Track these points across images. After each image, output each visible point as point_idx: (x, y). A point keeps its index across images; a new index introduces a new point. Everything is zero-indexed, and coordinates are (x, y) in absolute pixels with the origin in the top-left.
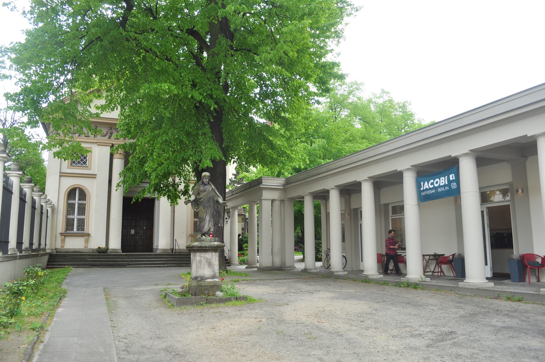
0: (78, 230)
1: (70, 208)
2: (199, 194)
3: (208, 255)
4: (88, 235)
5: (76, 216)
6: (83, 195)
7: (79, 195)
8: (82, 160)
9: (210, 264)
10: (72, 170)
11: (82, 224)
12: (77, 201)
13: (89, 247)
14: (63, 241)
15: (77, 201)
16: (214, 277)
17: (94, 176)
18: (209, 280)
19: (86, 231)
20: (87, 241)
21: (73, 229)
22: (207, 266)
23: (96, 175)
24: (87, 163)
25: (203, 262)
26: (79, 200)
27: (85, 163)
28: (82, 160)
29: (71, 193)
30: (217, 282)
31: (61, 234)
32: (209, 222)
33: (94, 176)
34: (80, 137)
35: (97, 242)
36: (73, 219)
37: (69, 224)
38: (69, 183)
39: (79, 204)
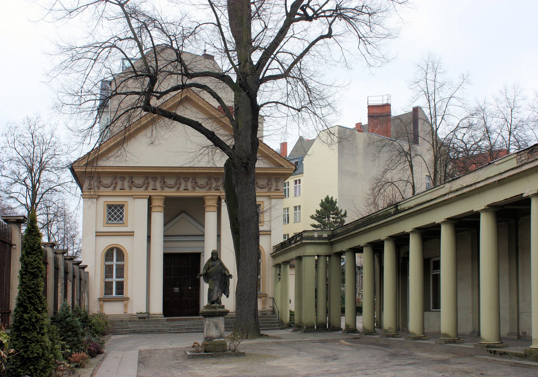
0: (118, 293)
1: (108, 271)
2: (209, 269)
3: (215, 320)
4: (127, 299)
5: (114, 279)
6: (121, 254)
7: (117, 256)
8: (118, 216)
9: (217, 327)
10: (108, 228)
11: (120, 287)
12: (115, 262)
13: (129, 312)
14: (101, 307)
15: (115, 262)
16: (221, 337)
17: (131, 234)
18: (216, 340)
19: (125, 295)
20: (126, 306)
21: (111, 293)
22: (214, 328)
23: (133, 232)
24: (124, 219)
25: (211, 326)
26: (117, 261)
27: (121, 219)
28: (118, 216)
29: (109, 254)
30: (222, 341)
31: (100, 300)
32: (218, 292)
33: (131, 234)
34: (115, 191)
36: (112, 283)
37: (108, 287)
38: (107, 242)
39: (117, 265)
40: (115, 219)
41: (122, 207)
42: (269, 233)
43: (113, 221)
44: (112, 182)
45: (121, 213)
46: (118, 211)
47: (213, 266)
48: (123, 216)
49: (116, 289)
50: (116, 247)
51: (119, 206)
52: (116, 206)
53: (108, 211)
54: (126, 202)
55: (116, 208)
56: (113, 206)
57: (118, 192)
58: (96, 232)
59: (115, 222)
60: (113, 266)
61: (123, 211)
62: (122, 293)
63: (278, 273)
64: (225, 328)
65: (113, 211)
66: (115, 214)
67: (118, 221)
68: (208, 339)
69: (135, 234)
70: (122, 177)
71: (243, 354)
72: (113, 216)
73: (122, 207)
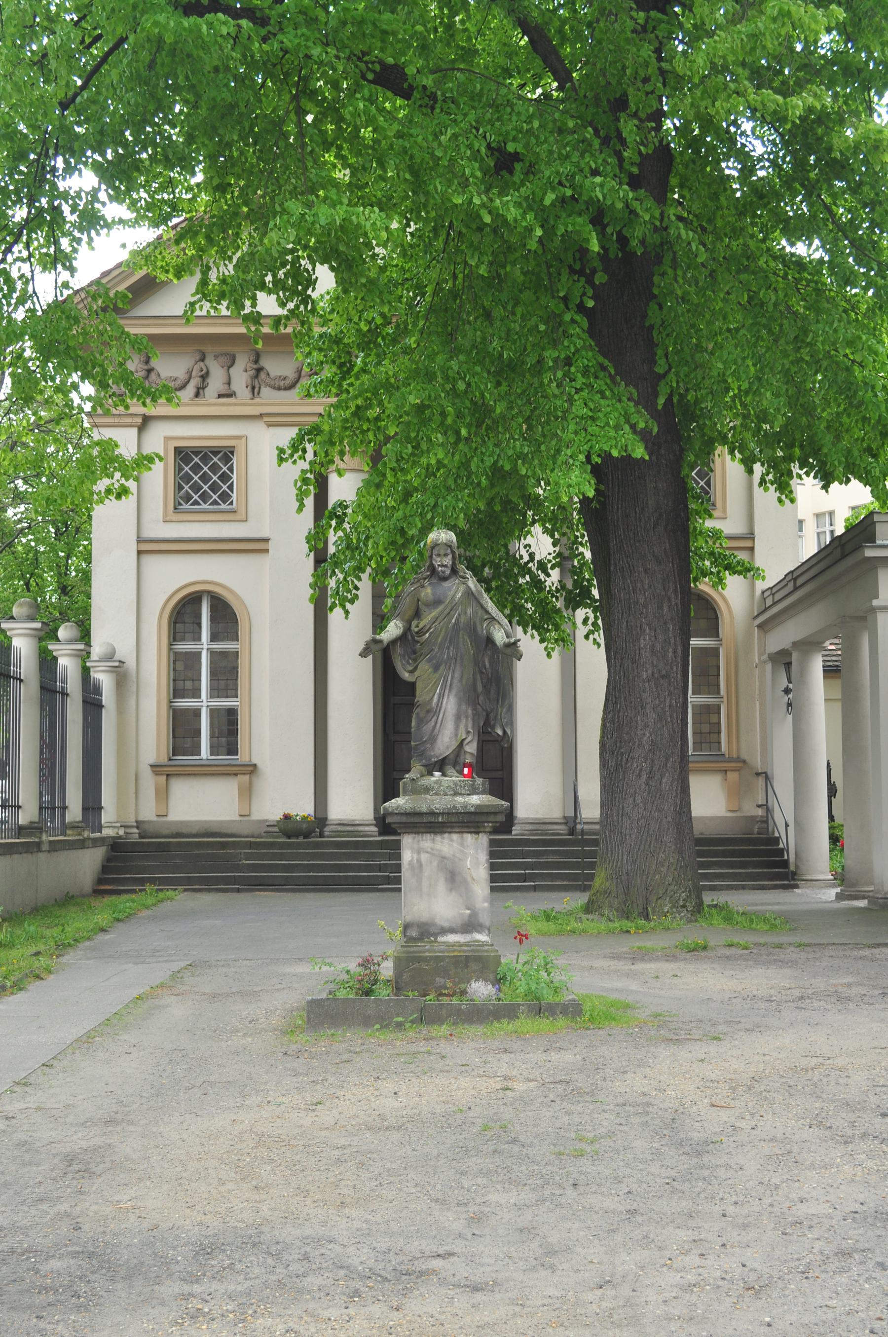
0: (214, 750)
1: (182, 676)
2: (417, 614)
3: (448, 845)
4: (252, 769)
5: (205, 702)
6: (226, 617)
7: (213, 619)
8: (214, 488)
9: (454, 878)
10: (181, 526)
11: (228, 727)
12: (205, 645)
13: (256, 816)
14: (163, 795)
15: (205, 645)
16: (470, 926)
17: (257, 546)
18: (451, 938)
19: (242, 757)
20: (247, 793)
21: (197, 750)
22: (441, 886)
23: (266, 540)
24: (234, 496)
25: (427, 872)
26: (214, 638)
27: (225, 497)
28: (214, 488)
29: (184, 613)
30: (484, 944)
31: (156, 768)
32: (458, 718)
33: (257, 546)
34: (199, 401)
35: (283, 796)
36: (197, 713)
37: (183, 729)
38: (173, 577)
39: (212, 653)
40: (204, 497)
41: (227, 454)
42: (748, 544)
43: (196, 503)
44: (190, 373)
45: (225, 478)
46: (214, 468)
47: (437, 602)
48: (231, 487)
49: (209, 738)
50: (208, 592)
51: (215, 451)
52: (206, 454)
53: (181, 469)
54: (239, 438)
55: (205, 459)
56: (196, 453)
57: (210, 405)
58: (140, 541)
59: (204, 506)
60: (198, 655)
61: (231, 469)
62: (233, 750)
63: (784, 683)
64: (493, 878)
65: (196, 468)
66: (205, 478)
67: (215, 503)
68: (414, 933)
69: (271, 546)
70: (226, 354)
71: (572, 1010)
72: (196, 488)
73: (227, 454)
